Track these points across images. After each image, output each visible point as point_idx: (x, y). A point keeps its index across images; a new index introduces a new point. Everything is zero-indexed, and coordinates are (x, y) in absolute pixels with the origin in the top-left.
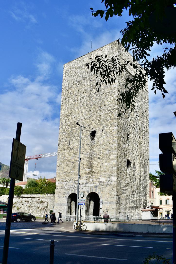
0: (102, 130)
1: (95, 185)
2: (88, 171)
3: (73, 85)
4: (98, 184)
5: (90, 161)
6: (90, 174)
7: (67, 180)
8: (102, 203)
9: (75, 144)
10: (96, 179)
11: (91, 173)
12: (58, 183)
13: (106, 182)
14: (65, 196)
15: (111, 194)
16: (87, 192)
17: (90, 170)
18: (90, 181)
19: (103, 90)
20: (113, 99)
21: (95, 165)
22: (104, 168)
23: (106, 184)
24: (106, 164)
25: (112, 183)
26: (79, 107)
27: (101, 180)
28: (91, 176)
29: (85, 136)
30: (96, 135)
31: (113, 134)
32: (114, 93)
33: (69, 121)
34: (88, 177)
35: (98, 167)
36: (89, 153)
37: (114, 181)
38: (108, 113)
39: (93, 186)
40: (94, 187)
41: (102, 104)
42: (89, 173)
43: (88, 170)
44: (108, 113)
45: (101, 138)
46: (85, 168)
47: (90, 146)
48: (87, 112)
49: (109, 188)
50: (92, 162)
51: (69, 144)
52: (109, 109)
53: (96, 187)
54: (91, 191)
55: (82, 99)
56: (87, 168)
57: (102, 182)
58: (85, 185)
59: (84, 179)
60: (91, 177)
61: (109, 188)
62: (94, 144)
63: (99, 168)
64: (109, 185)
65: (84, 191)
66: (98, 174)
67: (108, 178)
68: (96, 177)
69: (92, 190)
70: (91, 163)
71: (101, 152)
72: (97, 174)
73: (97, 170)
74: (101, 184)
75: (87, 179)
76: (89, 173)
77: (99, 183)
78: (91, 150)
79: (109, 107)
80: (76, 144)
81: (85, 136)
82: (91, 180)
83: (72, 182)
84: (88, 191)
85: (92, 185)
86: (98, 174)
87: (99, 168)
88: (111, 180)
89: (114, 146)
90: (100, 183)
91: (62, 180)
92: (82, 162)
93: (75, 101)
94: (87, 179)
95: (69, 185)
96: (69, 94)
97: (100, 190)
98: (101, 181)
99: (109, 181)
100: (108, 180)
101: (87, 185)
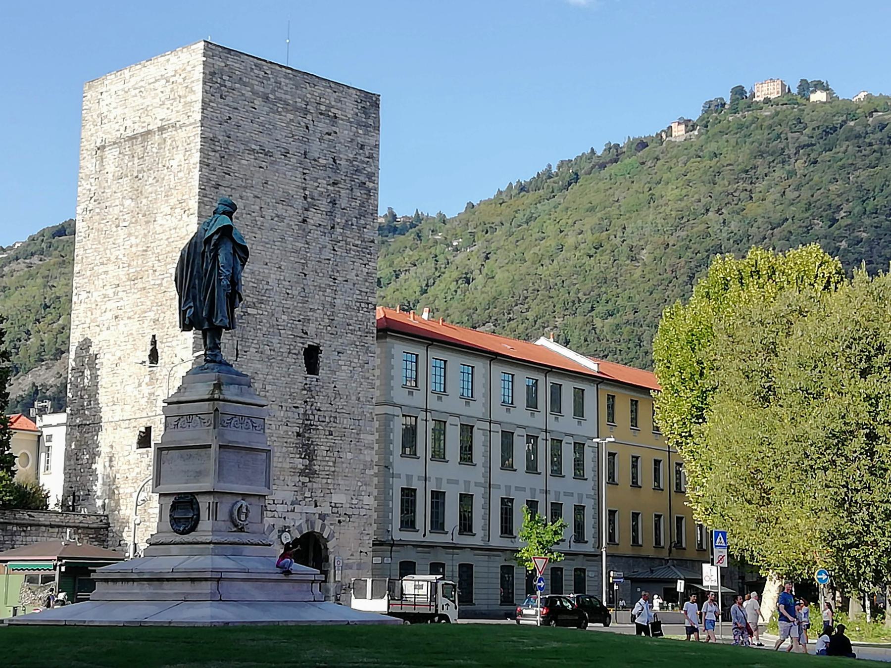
2: (300, 466)
3: (243, 147)
5: (307, 435)
11: (308, 472)
13: (348, 506)
15: (360, 541)
18: (305, 497)
19: (342, 231)
20: (367, 273)
21: (321, 451)
22: (344, 465)
24: (349, 456)
25: (363, 512)
26: (267, 244)
27: (336, 498)
28: (310, 481)
29: (289, 353)
31: (367, 375)
32: (368, 254)
34: (300, 484)
35: (327, 459)
41: (338, 271)
42: (302, 473)
43: (300, 463)
46: (291, 456)
47: (305, 389)
48: (295, 275)
49: (356, 524)
50: (312, 441)
53: (322, 517)
55: (276, 219)
56: (298, 456)
57: (337, 505)
58: (290, 508)
60: (309, 485)
61: (356, 524)
63: (331, 464)
64: (357, 516)
66: (329, 481)
69: (313, 527)
70: (310, 442)
71: (335, 418)
72: (325, 481)
73: (327, 468)
74: (335, 510)
75: (296, 489)
76: (302, 473)
78: (306, 402)
80: (260, 366)
81: (289, 353)
82: (307, 494)
84: (299, 528)
85: (311, 509)
86: (329, 481)
88: (361, 502)
89: (370, 411)
90: (332, 507)
92: (282, 433)
93: (253, 214)
94: (296, 489)
96: (229, 175)
97: (332, 527)
98: (335, 504)
100: (354, 502)
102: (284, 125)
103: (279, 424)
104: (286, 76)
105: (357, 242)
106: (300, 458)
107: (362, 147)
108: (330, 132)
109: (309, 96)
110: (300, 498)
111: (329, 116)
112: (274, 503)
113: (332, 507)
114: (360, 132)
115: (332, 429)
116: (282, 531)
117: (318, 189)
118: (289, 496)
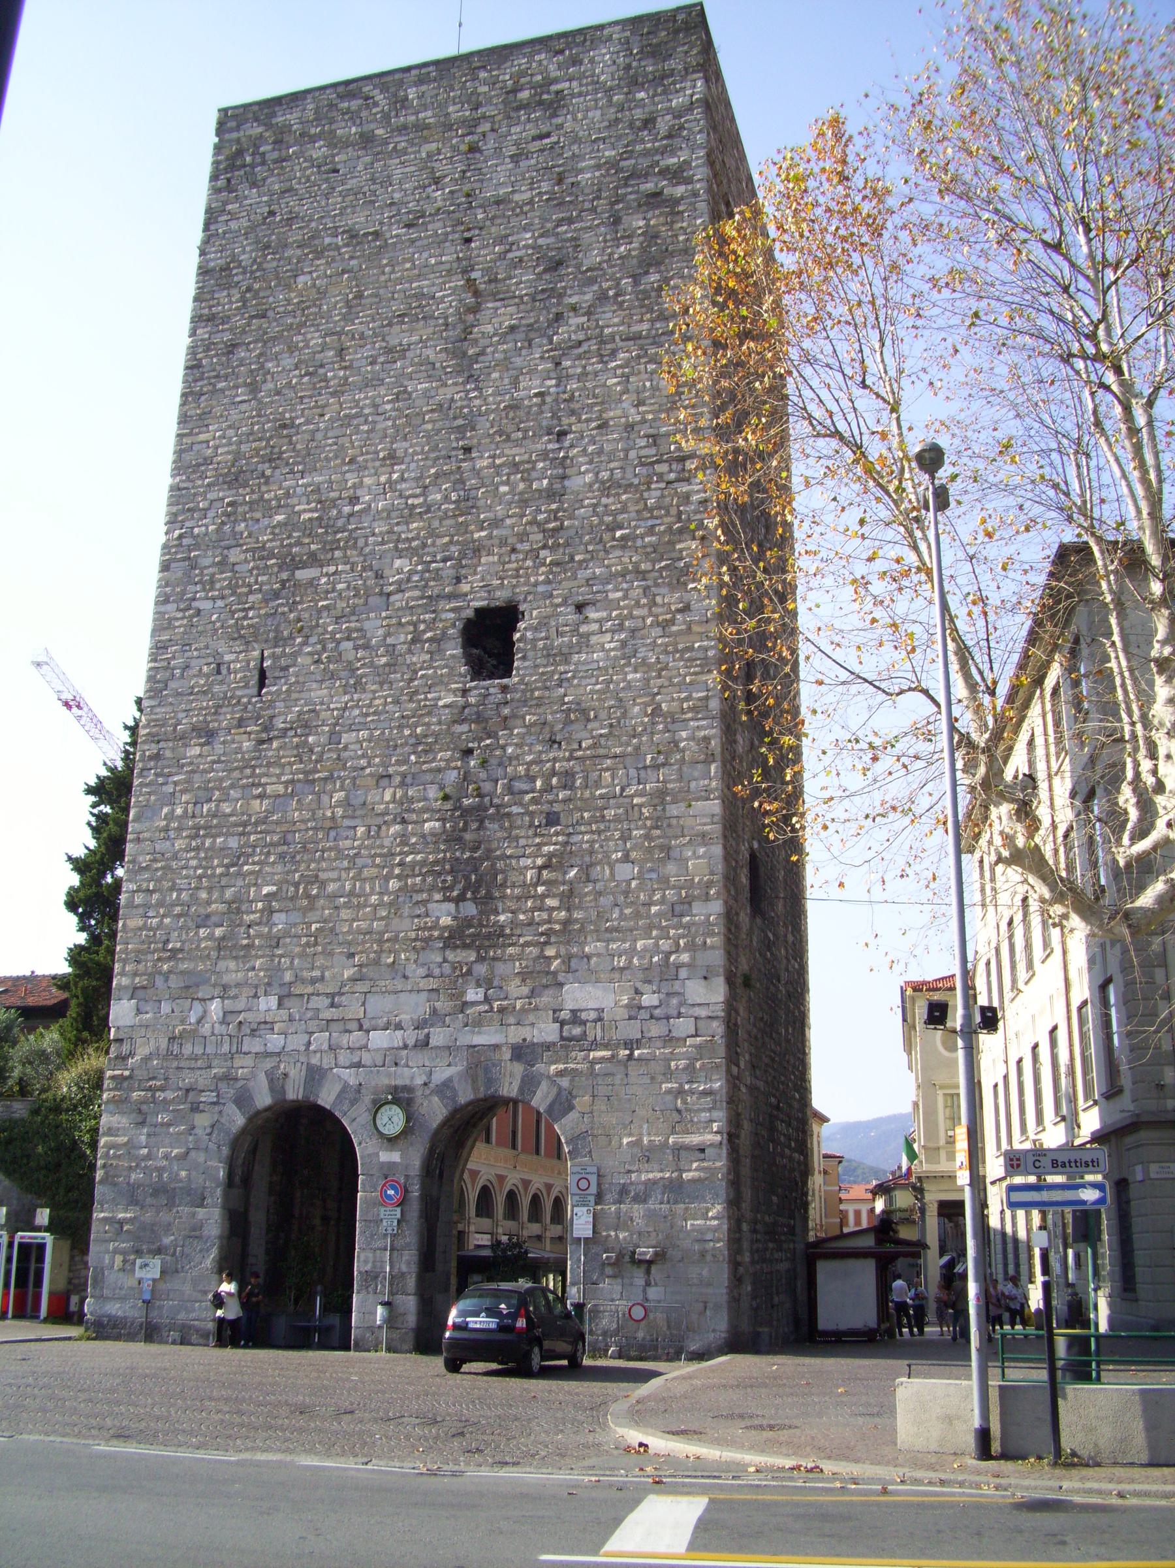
0: (580, 607)
1: (515, 1035)
4: (546, 1032)
6: (465, 946)
7: (225, 987)
8: (593, 1189)
9: (318, 693)
10: (525, 990)
12: (139, 1011)
14: (202, 1121)
16: (435, 1099)
17: (470, 909)
23: (632, 1031)
24: (625, 871)
28: (481, 959)
30: (523, 631)
33: (258, 515)
36: (452, 776)
37: (703, 1012)
38: (636, 481)
39: (496, 1047)
40: (507, 1055)
44: (631, 485)
45: (567, 661)
47: (463, 721)
51: (255, 691)
52: (643, 452)
54: (475, 1089)
57: (584, 1016)
58: (411, 1037)
59: (399, 984)
60: (481, 969)
62: (506, 711)
65: (408, 1089)
67: (646, 988)
68: (524, 976)
76: (454, 938)
77: (555, 1020)
79: (643, 442)
83: (280, 1005)
86: (550, 952)
87: (551, 902)
88: (674, 1001)
90: (563, 1023)
91: (174, 982)
94: (433, 984)
95: (246, 1030)
98: (573, 1012)
99: (657, 1012)
100: (649, 999)
101: (439, 1036)
102: (413, 169)
103: (379, 821)
104: (421, 81)
105: (636, 328)
106: (447, 899)
107: (649, 123)
108: (544, 129)
109: (485, 89)
110: (443, 1005)
111: (541, 103)
112: (361, 1028)
113: (563, 1023)
114: (642, 95)
115: (557, 808)
116: (378, 1106)
117: (510, 255)
118: (413, 1007)
